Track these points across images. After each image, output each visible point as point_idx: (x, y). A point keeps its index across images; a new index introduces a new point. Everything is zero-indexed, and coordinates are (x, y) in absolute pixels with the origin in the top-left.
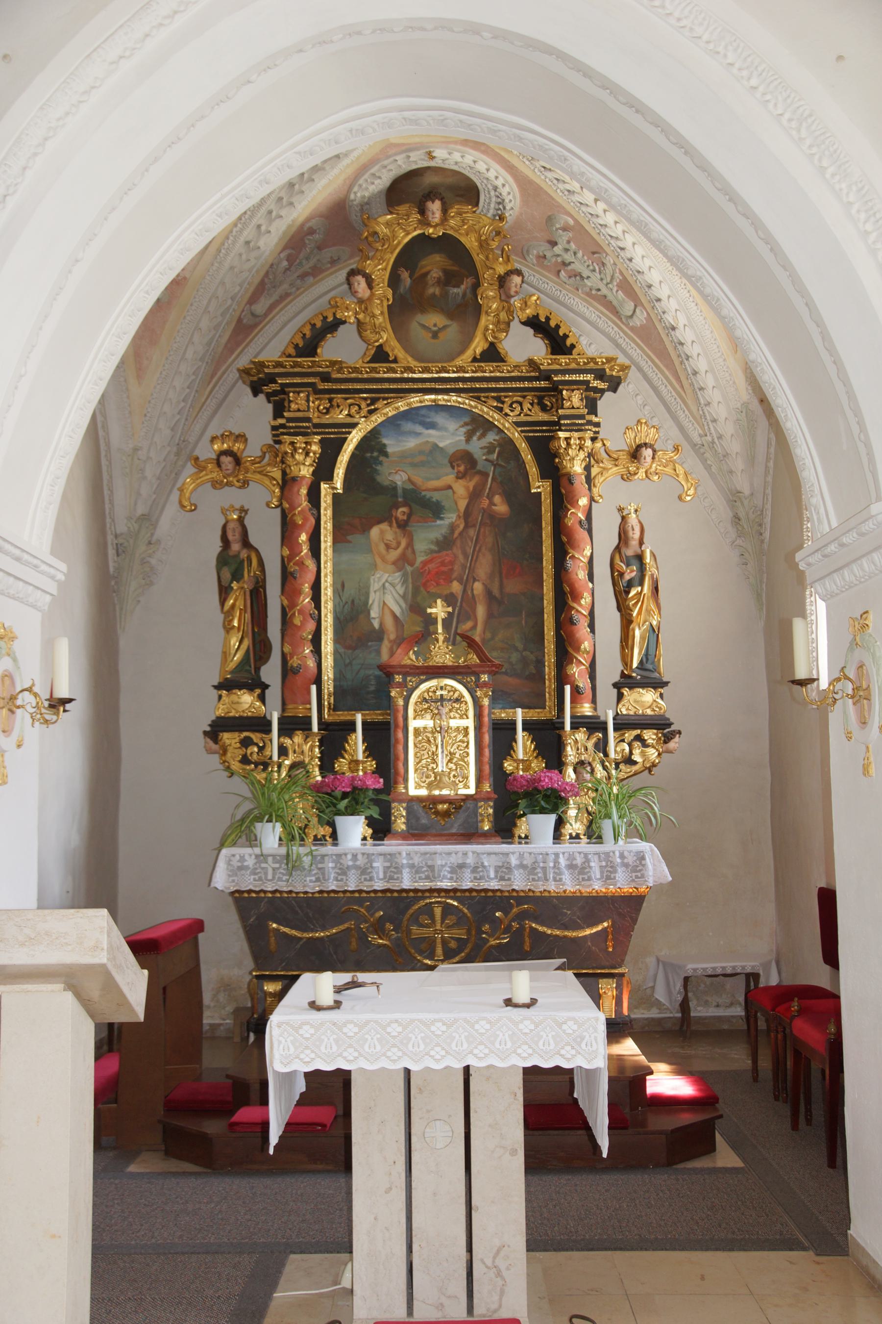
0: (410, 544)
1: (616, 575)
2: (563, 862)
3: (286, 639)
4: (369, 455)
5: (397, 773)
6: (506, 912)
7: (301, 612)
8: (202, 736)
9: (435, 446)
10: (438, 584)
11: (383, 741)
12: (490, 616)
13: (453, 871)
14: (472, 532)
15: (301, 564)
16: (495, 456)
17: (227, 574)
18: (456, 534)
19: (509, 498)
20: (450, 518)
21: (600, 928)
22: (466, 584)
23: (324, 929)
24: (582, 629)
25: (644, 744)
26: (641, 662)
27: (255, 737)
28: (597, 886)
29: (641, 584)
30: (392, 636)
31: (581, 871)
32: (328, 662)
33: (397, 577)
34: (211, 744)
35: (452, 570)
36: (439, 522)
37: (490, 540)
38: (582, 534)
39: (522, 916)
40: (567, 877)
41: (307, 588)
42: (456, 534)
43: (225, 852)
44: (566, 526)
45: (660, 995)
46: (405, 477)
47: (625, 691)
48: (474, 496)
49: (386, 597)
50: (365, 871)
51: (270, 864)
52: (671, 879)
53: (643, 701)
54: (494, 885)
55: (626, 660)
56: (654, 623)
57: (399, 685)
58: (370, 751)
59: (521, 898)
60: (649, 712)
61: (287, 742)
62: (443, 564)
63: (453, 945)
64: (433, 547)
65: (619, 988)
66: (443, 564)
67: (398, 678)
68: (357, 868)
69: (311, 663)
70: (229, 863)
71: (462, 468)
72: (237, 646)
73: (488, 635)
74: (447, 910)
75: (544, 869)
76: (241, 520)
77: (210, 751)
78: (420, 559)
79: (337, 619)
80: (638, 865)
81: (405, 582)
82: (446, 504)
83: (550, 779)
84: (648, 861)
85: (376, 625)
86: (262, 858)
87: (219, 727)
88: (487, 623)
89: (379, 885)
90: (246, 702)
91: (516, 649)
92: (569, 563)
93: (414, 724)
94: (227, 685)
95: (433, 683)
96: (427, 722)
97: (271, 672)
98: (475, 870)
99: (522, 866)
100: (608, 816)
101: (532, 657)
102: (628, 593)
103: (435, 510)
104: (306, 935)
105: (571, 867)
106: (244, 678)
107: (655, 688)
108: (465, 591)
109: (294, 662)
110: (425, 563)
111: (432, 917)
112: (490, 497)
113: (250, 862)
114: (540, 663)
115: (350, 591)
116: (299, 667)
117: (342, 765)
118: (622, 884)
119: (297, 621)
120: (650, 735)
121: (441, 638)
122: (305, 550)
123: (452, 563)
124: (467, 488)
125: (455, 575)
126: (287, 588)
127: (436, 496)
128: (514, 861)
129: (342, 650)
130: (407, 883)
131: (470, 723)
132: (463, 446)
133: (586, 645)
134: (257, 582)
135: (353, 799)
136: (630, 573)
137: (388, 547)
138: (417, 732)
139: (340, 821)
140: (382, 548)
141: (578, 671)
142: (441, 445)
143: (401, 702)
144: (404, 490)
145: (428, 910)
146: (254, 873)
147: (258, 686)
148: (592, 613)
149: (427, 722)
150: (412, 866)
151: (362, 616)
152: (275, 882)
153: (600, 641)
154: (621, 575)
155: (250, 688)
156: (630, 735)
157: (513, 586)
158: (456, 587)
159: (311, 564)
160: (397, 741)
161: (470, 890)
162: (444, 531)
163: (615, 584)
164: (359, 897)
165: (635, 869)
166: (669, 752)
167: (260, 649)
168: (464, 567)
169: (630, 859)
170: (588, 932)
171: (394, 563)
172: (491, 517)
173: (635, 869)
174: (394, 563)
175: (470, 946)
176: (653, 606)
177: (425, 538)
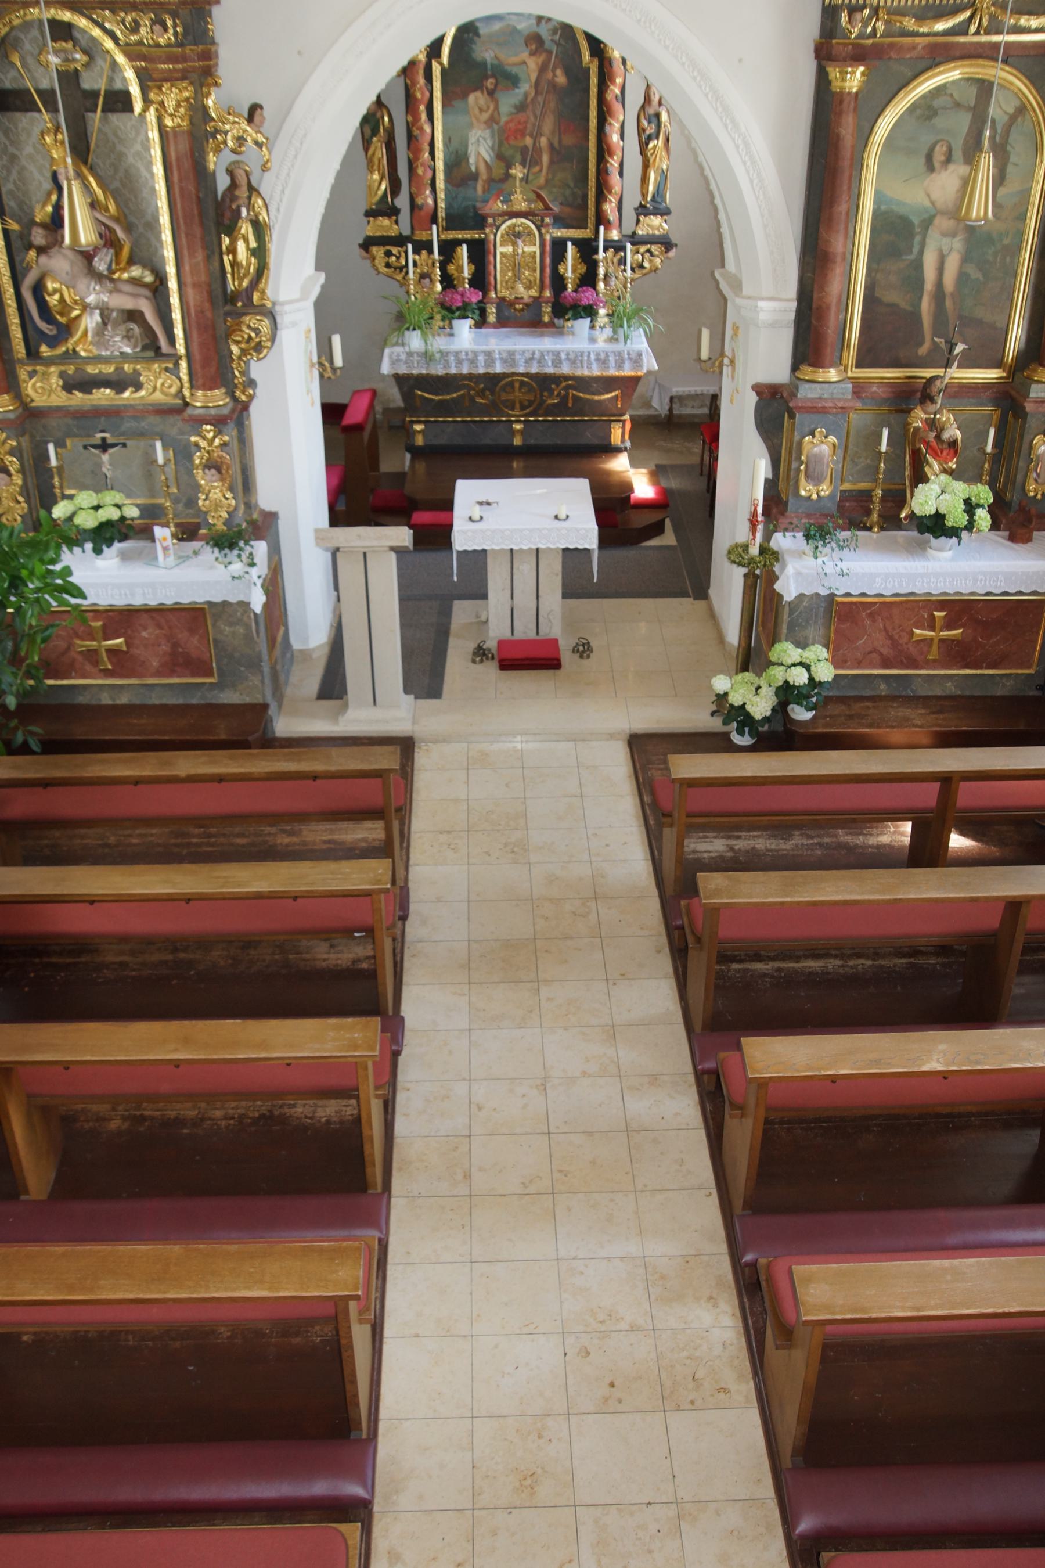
0: (497, 108)
1: (641, 130)
2: (593, 357)
3: (413, 184)
4: (466, 35)
5: (489, 283)
6: (558, 386)
7: (422, 165)
8: (357, 247)
9: (515, 29)
10: (516, 138)
11: (479, 252)
12: (552, 162)
13: (526, 362)
14: (540, 99)
15: (421, 129)
16: (557, 37)
17: (368, 131)
18: (529, 100)
19: (567, 72)
20: (526, 87)
21: (613, 394)
22: (536, 139)
23: (448, 394)
24: (615, 179)
25: (652, 255)
26: (653, 196)
27: (395, 250)
28: (613, 372)
29: (657, 138)
30: (485, 177)
31: (604, 363)
32: (441, 195)
33: (487, 133)
34: (364, 254)
35: (525, 128)
36: (517, 91)
37: (552, 105)
38: (617, 107)
40: (595, 366)
41: (426, 147)
42: (529, 100)
43: (387, 351)
44: (606, 99)
45: (655, 403)
46: (492, 55)
47: (642, 218)
48: (543, 69)
49: (480, 149)
50: (473, 362)
51: (416, 358)
52: (656, 368)
53: (655, 225)
54: (550, 370)
55: (644, 196)
56: (665, 167)
57: (491, 225)
58: (471, 259)
59: (566, 378)
60: (657, 233)
61: (417, 257)
62: (519, 123)
63: (526, 403)
64: (514, 111)
65: (623, 428)
66: (519, 123)
67: (490, 220)
68: (468, 360)
69: (430, 201)
70: (390, 357)
71: (534, 47)
73: (550, 176)
74: (522, 383)
75: (582, 362)
77: (364, 258)
78: (504, 119)
79: (446, 164)
80: (637, 360)
81: (493, 137)
82: (522, 76)
83: (587, 296)
84: (644, 356)
85: (473, 169)
86: (410, 354)
87: (368, 244)
88: (549, 168)
89: (481, 371)
90: (384, 226)
91: (569, 187)
92: (607, 128)
93: (500, 249)
94: (371, 214)
95: (514, 220)
96: (510, 249)
97: (402, 202)
98: (539, 362)
99: (568, 359)
100: (622, 326)
101: (580, 193)
102: (647, 144)
103: (513, 81)
104: (437, 398)
105: (598, 360)
106: (385, 209)
107: (662, 215)
108: (534, 144)
109: (419, 201)
110: (507, 123)
111: (513, 387)
112: (553, 71)
113: (403, 357)
114: (585, 197)
115: (455, 144)
116: (423, 205)
117: (451, 268)
118: (627, 372)
119: (420, 171)
120: (654, 248)
121: (518, 190)
122: (424, 117)
123: (526, 122)
124: (537, 64)
125: (528, 131)
126: (412, 146)
127: (515, 70)
128: (563, 356)
129: (450, 187)
130: (498, 368)
131: (536, 249)
132: (535, 29)
133: (617, 189)
134: (389, 135)
135: (463, 312)
136: (650, 130)
137: (481, 110)
138: (501, 253)
139: (455, 322)
140: (477, 111)
141: (610, 208)
142: (519, 27)
143: (492, 237)
144: (492, 65)
145: (511, 384)
146: (406, 363)
147: (392, 212)
148: (621, 165)
149: (510, 249)
150: (501, 359)
151: (463, 164)
152: (418, 369)
153: (625, 186)
154: (644, 130)
155: (389, 216)
156: (643, 249)
157: (569, 140)
158: (528, 141)
159: (427, 129)
160: (489, 263)
161: (537, 373)
162: (521, 97)
163: (639, 136)
164: (470, 377)
165: (636, 362)
166: (668, 258)
167: (395, 186)
168: (534, 125)
169: (633, 356)
170: (606, 396)
171: (485, 123)
172: (553, 85)
173: (636, 362)
174: (485, 123)
175: (535, 406)
176: (664, 154)
177: (508, 102)
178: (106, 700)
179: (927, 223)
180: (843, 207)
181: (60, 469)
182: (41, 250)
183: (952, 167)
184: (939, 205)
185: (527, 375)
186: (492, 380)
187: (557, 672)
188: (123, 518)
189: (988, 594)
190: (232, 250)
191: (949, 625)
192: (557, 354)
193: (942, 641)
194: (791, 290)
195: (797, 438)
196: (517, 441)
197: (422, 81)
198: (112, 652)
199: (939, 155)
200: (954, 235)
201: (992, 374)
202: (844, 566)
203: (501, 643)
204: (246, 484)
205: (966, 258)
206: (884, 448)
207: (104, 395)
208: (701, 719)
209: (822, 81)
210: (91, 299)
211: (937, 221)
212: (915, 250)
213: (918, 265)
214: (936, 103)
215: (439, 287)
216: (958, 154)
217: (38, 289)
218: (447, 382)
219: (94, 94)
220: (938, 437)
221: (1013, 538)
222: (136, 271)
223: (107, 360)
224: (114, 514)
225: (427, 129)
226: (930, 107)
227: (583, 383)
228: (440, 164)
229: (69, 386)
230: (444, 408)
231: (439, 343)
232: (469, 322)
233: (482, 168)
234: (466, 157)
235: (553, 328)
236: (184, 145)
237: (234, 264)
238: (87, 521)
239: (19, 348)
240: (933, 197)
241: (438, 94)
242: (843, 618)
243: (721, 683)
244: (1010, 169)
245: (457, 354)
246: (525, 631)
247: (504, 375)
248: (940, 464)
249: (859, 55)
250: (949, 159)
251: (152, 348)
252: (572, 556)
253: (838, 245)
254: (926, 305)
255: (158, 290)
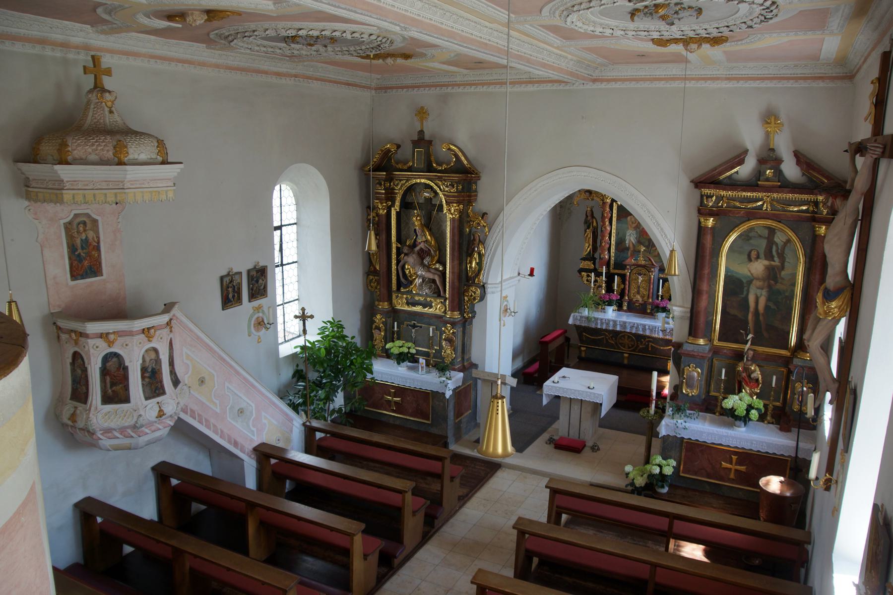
33: (634, 232)
39: (649, 341)
40: (661, 333)
50: (608, 324)
54: (641, 333)
59: (649, 337)
72: (587, 248)
74: (629, 337)
76: (592, 211)
87: (581, 271)
106: (591, 258)
122: (607, 223)
130: (618, 328)
159: (608, 228)
164: (606, 330)
167: (595, 249)
178: (391, 422)
179: (750, 282)
180: (706, 271)
181: (398, 332)
182: (406, 254)
183: (759, 260)
184: (755, 275)
185: (630, 333)
186: (615, 334)
187: (578, 455)
188: (409, 352)
189: (758, 451)
190: (471, 263)
191: (739, 463)
192: (644, 326)
193: (736, 470)
194: (689, 305)
195: (682, 366)
196: (626, 362)
197: (608, 209)
198: (396, 402)
199: (754, 254)
200: (762, 289)
201: (783, 352)
202: (687, 425)
203: (561, 438)
204: (465, 349)
205: (769, 299)
206: (723, 377)
207: (418, 309)
208: (621, 483)
209: (700, 222)
210: (419, 273)
211: (754, 282)
212: (745, 293)
213: (746, 300)
214: (751, 234)
215: (604, 292)
216: (762, 255)
217: (403, 267)
218: (596, 331)
219: (435, 205)
220: (749, 376)
221: (781, 429)
222: (437, 266)
223: (421, 295)
224: (406, 350)
225: (608, 228)
226: (748, 236)
227: (655, 340)
228: (613, 242)
229: (408, 304)
230: (594, 342)
231: (599, 315)
232: (614, 307)
233: (631, 246)
234: (625, 241)
235: (652, 315)
236: (456, 224)
237: (471, 267)
238: (395, 351)
239: (394, 287)
240: (753, 271)
241: (615, 215)
242: (690, 450)
243: (628, 468)
244: (786, 264)
245: (602, 319)
246: (574, 435)
247: (620, 332)
248: (750, 389)
249: (711, 214)
250: (758, 257)
251: (438, 294)
252: (597, 406)
253: (705, 287)
254: (750, 317)
255: (443, 274)
